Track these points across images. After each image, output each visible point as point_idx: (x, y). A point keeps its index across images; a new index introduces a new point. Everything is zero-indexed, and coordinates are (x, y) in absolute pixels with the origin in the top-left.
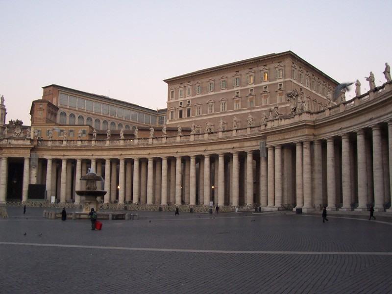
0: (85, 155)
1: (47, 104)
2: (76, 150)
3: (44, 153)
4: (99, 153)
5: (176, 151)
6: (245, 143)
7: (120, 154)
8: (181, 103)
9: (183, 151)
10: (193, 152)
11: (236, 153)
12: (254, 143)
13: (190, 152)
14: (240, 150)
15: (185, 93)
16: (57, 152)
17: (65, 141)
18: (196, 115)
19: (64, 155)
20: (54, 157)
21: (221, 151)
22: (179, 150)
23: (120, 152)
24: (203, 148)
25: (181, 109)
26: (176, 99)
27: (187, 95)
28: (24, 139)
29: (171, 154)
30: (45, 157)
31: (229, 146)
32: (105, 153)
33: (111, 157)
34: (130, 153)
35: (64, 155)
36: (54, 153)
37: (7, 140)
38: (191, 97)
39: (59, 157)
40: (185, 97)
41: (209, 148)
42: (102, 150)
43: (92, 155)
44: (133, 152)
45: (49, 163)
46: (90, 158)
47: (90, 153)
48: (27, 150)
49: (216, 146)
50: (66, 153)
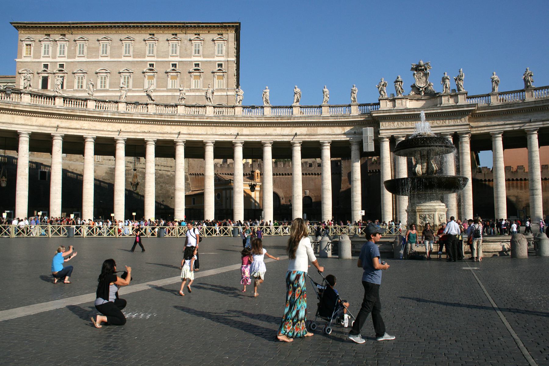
5: (177, 131)
6: (319, 128)
7: (56, 125)
8: (46, 66)
9: (191, 132)
10: (213, 135)
11: (355, 142)
12: (338, 130)
13: (207, 134)
14: (307, 139)
15: (54, 52)
18: (76, 87)
21: (270, 137)
22: (184, 129)
23: (55, 122)
24: (234, 130)
25: (46, 75)
26: (34, 58)
27: (58, 54)
29: (165, 135)
31: (287, 131)
32: (20, 119)
33: (36, 130)
34: (78, 127)
38: (65, 59)
40: (54, 57)
41: (246, 131)
44: (85, 124)
49: (259, 129)
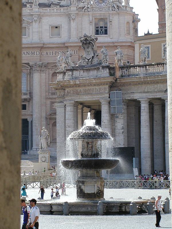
3: (134, 88)
16: (156, 86)
20: (151, 96)
28: (98, 69)
30: (136, 96)
36: (150, 87)
37: (71, 73)
45: (144, 107)
48: (102, 87)
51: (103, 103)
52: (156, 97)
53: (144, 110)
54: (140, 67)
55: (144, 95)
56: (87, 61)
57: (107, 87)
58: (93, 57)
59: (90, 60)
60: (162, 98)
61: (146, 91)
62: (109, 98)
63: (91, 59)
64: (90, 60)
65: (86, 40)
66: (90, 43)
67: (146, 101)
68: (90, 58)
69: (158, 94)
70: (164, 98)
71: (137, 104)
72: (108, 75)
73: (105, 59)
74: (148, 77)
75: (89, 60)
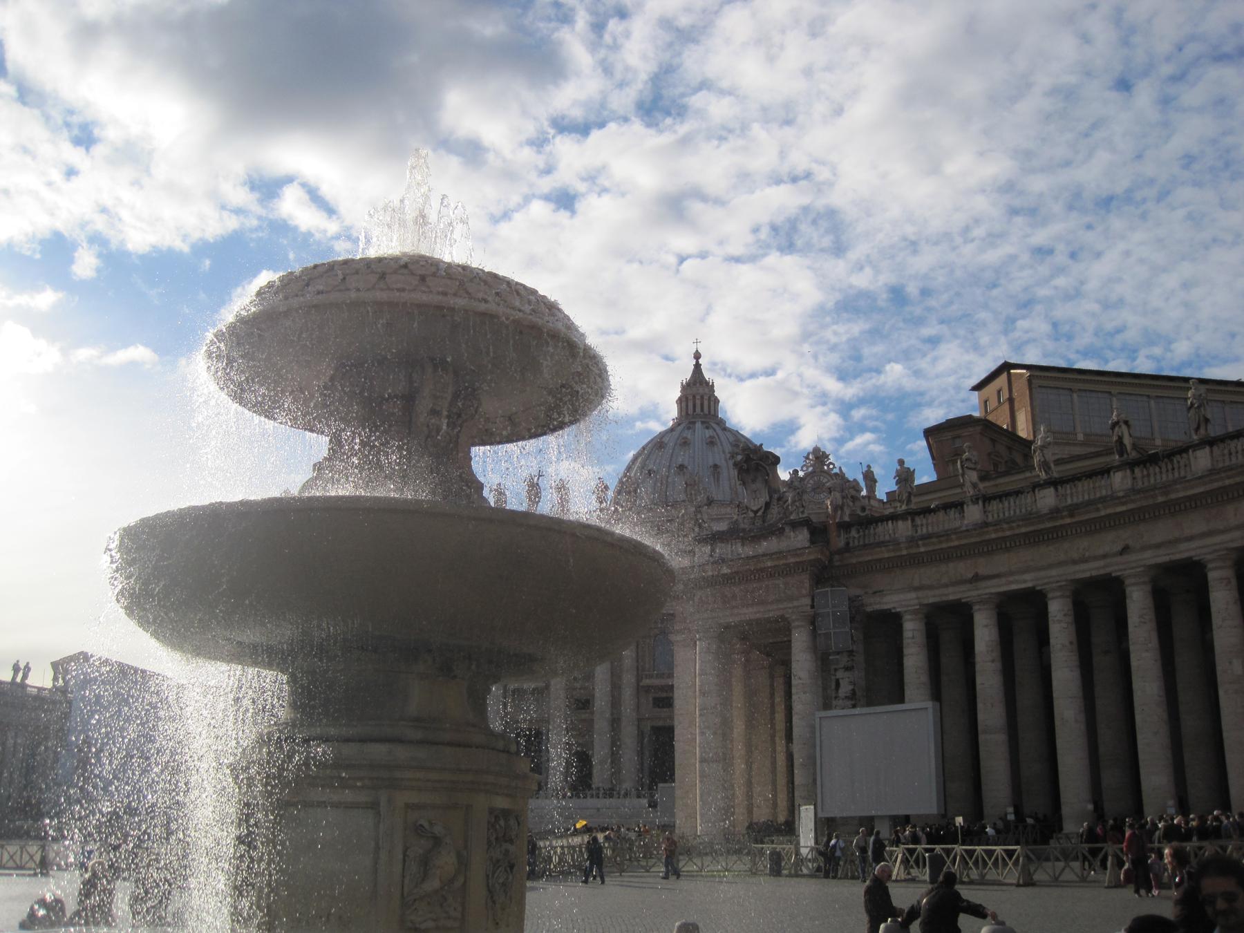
0: (1084, 560)
1: (978, 429)
2: (1035, 539)
4: (1161, 531)
17: (975, 500)
19: (977, 578)
20: (932, 597)
30: (890, 602)
32: (1195, 523)
35: (977, 578)
39: (952, 594)
42: (1175, 508)
43: (1126, 550)
45: (912, 629)
46: (1115, 567)
47: (1109, 542)
50: (984, 566)
51: (797, 623)
52: (944, 599)
53: (913, 638)
54: (897, 521)
55: (913, 595)
56: (752, 515)
57: (806, 579)
58: (767, 505)
59: (760, 513)
60: (963, 601)
61: (916, 583)
62: (813, 607)
63: (763, 509)
64: (760, 513)
65: (748, 459)
66: (758, 468)
67: (915, 612)
68: (761, 508)
69: (951, 589)
70: (968, 599)
71: (892, 621)
72: (807, 544)
73: (797, 504)
74: (920, 542)
75: (756, 512)
